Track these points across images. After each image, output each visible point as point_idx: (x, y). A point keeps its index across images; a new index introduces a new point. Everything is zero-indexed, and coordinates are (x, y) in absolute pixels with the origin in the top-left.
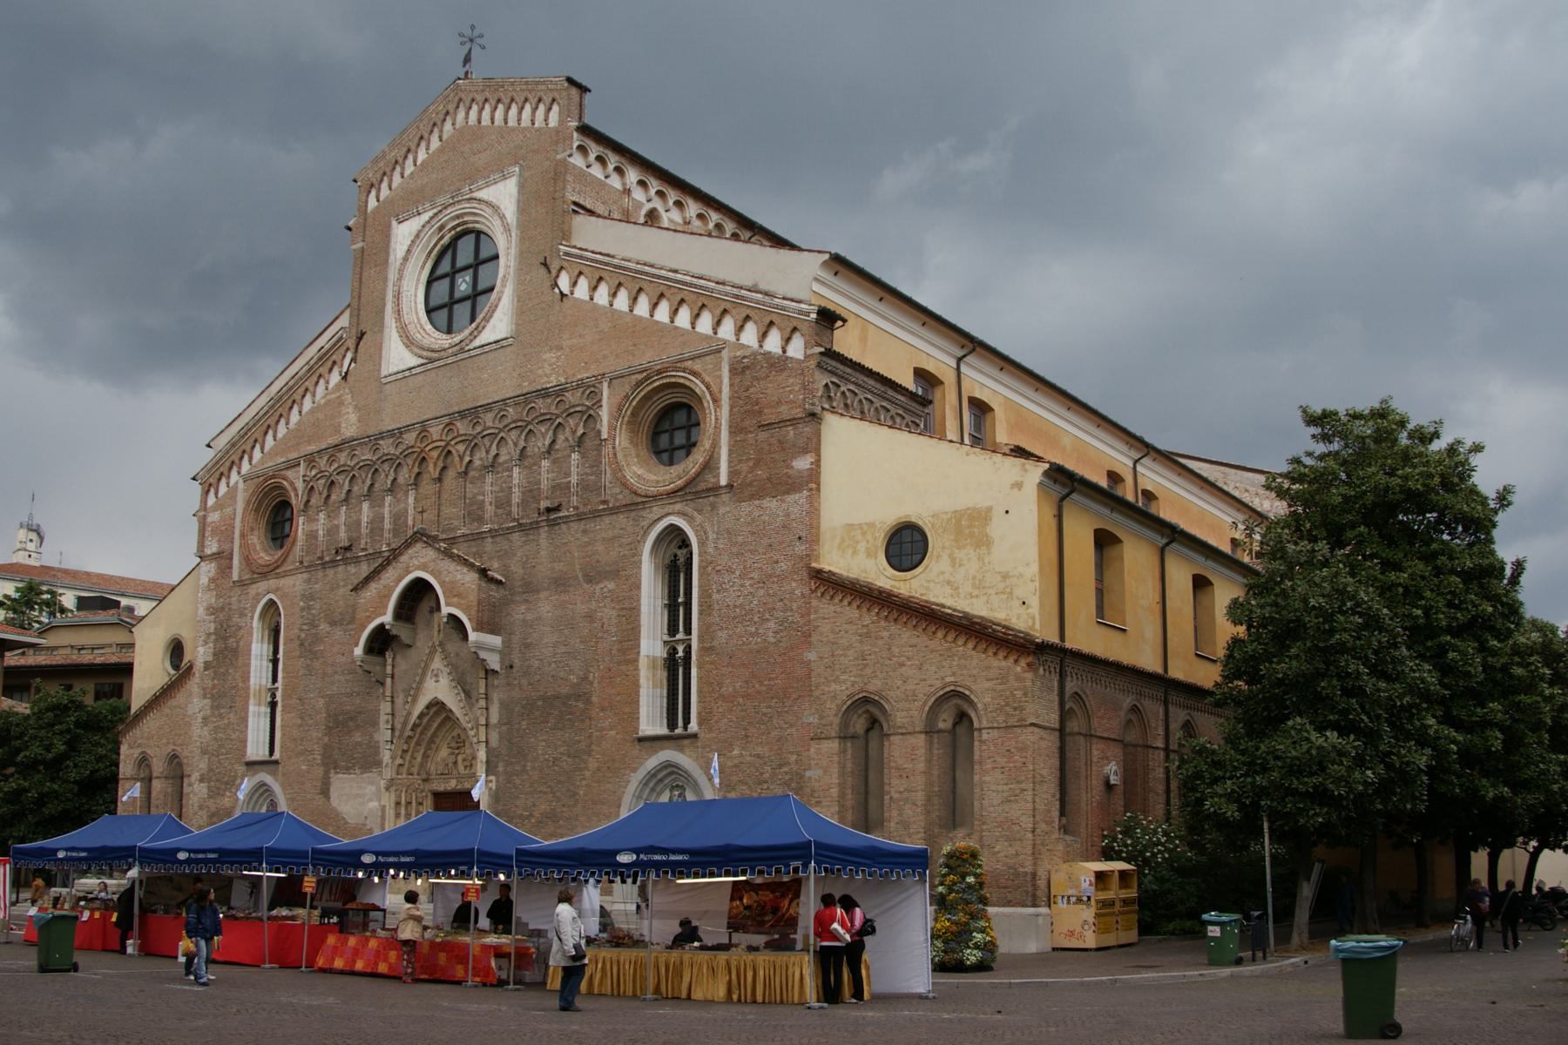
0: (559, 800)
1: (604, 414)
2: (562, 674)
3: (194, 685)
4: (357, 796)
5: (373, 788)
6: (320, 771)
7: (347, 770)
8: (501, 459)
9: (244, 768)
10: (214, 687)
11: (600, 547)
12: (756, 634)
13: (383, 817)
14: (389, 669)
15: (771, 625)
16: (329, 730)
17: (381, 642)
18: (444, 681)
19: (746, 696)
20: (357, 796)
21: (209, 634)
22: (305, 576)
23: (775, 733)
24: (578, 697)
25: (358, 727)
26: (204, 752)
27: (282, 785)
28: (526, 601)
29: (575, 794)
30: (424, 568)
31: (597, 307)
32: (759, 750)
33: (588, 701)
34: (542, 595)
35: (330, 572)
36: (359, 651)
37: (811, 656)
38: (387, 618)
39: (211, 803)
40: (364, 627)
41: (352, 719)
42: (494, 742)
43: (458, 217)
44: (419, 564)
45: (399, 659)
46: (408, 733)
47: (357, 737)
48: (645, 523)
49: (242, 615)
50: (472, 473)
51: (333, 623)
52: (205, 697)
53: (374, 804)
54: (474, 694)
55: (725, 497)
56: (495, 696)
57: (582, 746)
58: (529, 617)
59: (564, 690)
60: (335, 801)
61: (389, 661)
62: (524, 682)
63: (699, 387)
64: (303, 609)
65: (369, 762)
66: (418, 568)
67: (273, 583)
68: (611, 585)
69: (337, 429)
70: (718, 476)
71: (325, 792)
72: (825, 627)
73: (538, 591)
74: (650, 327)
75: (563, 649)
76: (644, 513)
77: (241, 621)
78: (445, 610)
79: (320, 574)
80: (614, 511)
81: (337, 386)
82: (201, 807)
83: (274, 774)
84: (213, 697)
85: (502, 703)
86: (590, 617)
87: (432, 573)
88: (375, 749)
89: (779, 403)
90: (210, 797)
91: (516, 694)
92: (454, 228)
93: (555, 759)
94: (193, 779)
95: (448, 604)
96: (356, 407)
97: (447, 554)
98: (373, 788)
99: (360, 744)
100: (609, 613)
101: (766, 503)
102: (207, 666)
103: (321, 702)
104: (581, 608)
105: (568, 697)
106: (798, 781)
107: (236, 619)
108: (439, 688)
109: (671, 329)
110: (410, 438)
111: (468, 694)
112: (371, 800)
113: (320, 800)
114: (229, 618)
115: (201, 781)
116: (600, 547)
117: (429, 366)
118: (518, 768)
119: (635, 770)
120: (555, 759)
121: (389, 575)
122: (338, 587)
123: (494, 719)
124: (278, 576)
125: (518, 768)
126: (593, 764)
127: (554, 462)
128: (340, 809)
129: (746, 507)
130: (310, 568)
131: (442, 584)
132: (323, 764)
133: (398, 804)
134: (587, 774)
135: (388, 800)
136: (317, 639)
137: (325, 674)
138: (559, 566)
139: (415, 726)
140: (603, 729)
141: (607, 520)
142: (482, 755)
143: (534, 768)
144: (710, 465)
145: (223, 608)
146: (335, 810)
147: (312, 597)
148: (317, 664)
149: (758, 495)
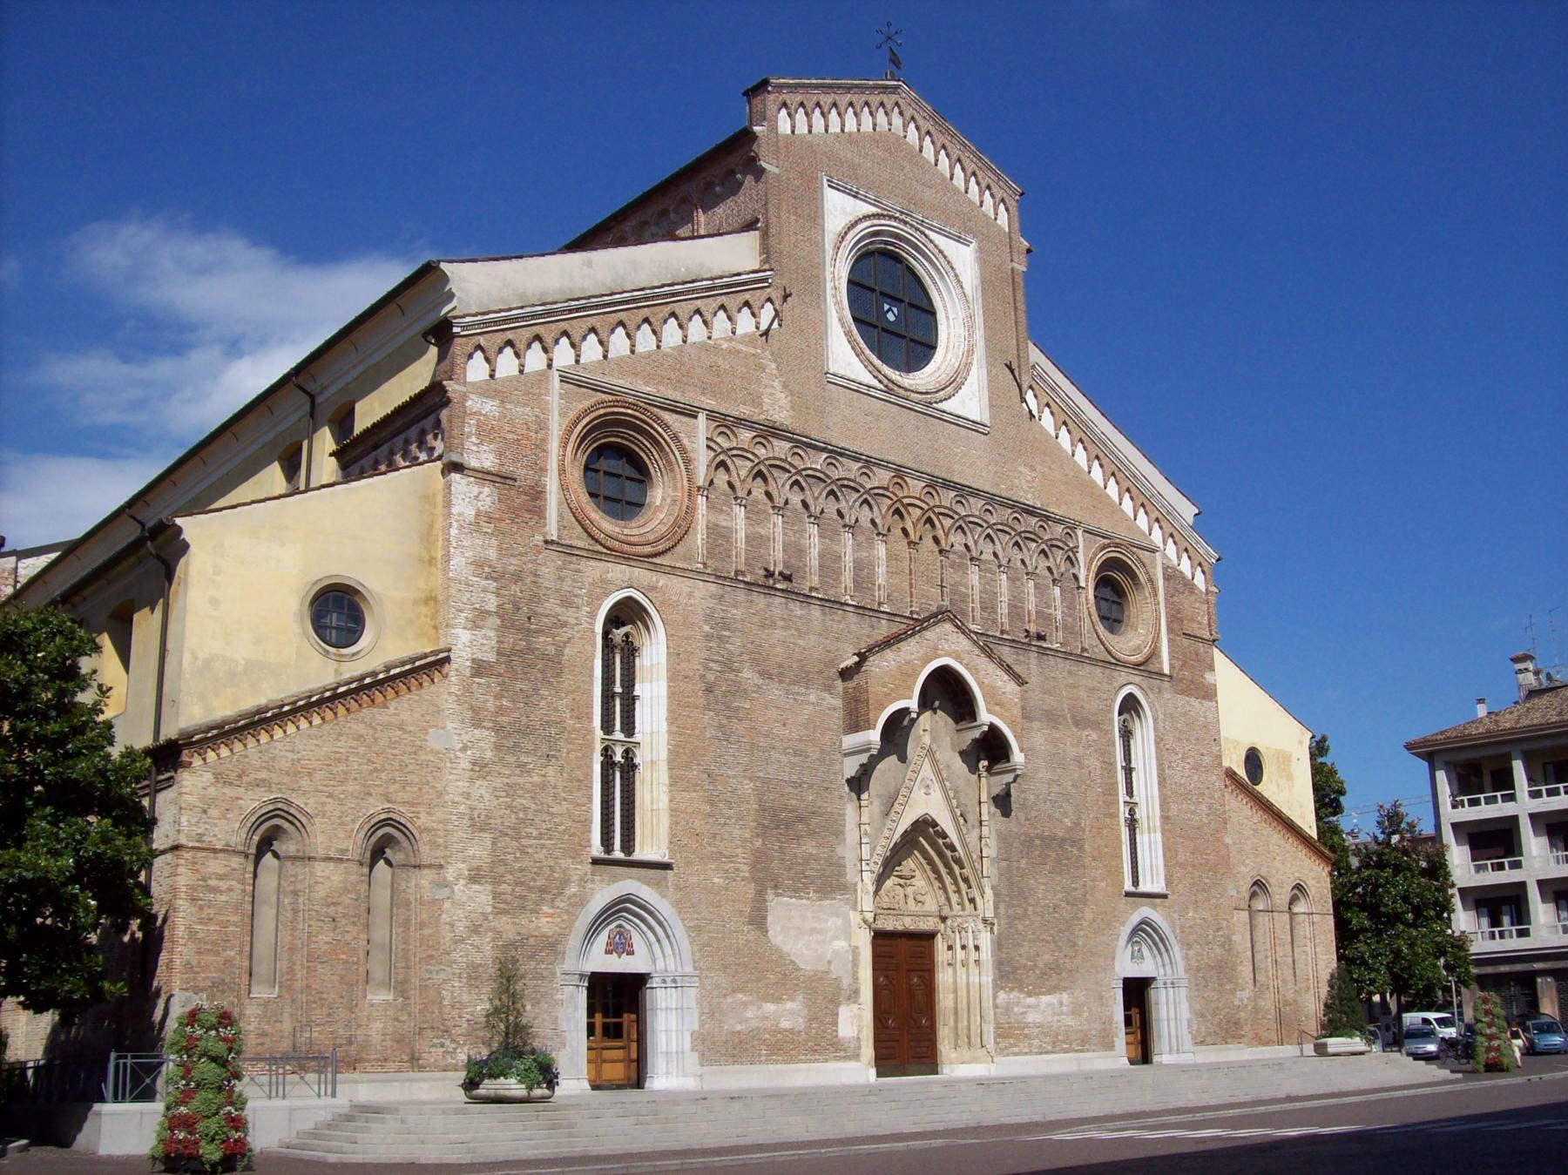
0: (1061, 950)
1: (1081, 556)
2: (1057, 815)
3: (445, 692)
4: (813, 931)
5: (839, 922)
6: (750, 889)
7: (797, 891)
9: (588, 868)
10: (500, 711)
11: (1083, 694)
12: (1194, 813)
13: (855, 964)
15: (1203, 807)
16: (762, 830)
18: (937, 794)
19: (1193, 866)
20: (813, 931)
21: (483, 614)
22: (713, 588)
23: (1213, 901)
24: (1073, 842)
25: (812, 834)
26: (479, 825)
27: (677, 904)
29: (1075, 944)
30: (957, 658)
31: (1059, 448)
32: (1206, 915)
33: (1081, 849)
35: (760, 600)
37: (1228, 840)
38: (913, 704)
39: (505, 925)
41: (800, 819)
43: (897, 236)
44: (948, 649)
47: (810, 847)
48: (1117, 685)
49: (566, 602)
51: (765, 674)
52: (477, 724)
53: (841, 944)
55: (1167, 685)
57: (1078, 894)
59: (1060, 834)
60: (778, 932)
63: (1142, 577)
64: (708, 637)
65: (832, 884)
66: (950, 655)
67: (640, 574)
68: (1094, 736)
69: (756, 400)
70: (1161, 663)
71: (758, 920)
72: (1235, 819)
74: (1100, 497)
75: (1055, 789)
76: (1116, 674)
77: (569, 615)
79: (741, 595)
80: (1094, 662)
81: (748, 339)
82: (475, 929)
83: (658, 885)
84: (498, 729)
86: (1079, 761)
87: (966, 666)
88: (838, 867)
89: (1192, 620)
90: (499, 912)
92: (887, 243)
93: (1056, 906)
94: (450, 873)
95: (989, 711)
96: (785, 386)
97: (987, 651)
98: (839, 922)
100: (1093, 763)
101: (1192, 700)
102: (479, 668)
103: (748, 787)
104: (1071, 751)
105: (1063, 840)
106: (1228, 945)
107: (551, 605)
108: (927, 801)
109: (1117, 508)
110: (882, 477)
112: (835, 938)
113: (751, 934)
114: (534, 598)
115: (475, 877)
116: (1083, 694)
117: (893, 399)
118: (1020, 911)
119: (1123, 924)
120: (1056, 906)
121: (910, 648)
122: (773, 625)
123: (994, 854)
124: (655, 568)
126: (1088, 916)
127: (1036, 586)
128: (786, 948)
129: (1181, 700)
130: (719, 577)
131: (981, 684)
132: (754, 879)
134: (1085, 924)
136: (737, 690)
137: (753, 747)
138: (1049, 700)
140: (1094, 880)
141: (1088, 668)
143: (1035, 913)
144: (1154, 653)
145: (518, 577)
146: (778, 950)
147: (726, 627)
148: (739, 728)
149: (1186, 692)
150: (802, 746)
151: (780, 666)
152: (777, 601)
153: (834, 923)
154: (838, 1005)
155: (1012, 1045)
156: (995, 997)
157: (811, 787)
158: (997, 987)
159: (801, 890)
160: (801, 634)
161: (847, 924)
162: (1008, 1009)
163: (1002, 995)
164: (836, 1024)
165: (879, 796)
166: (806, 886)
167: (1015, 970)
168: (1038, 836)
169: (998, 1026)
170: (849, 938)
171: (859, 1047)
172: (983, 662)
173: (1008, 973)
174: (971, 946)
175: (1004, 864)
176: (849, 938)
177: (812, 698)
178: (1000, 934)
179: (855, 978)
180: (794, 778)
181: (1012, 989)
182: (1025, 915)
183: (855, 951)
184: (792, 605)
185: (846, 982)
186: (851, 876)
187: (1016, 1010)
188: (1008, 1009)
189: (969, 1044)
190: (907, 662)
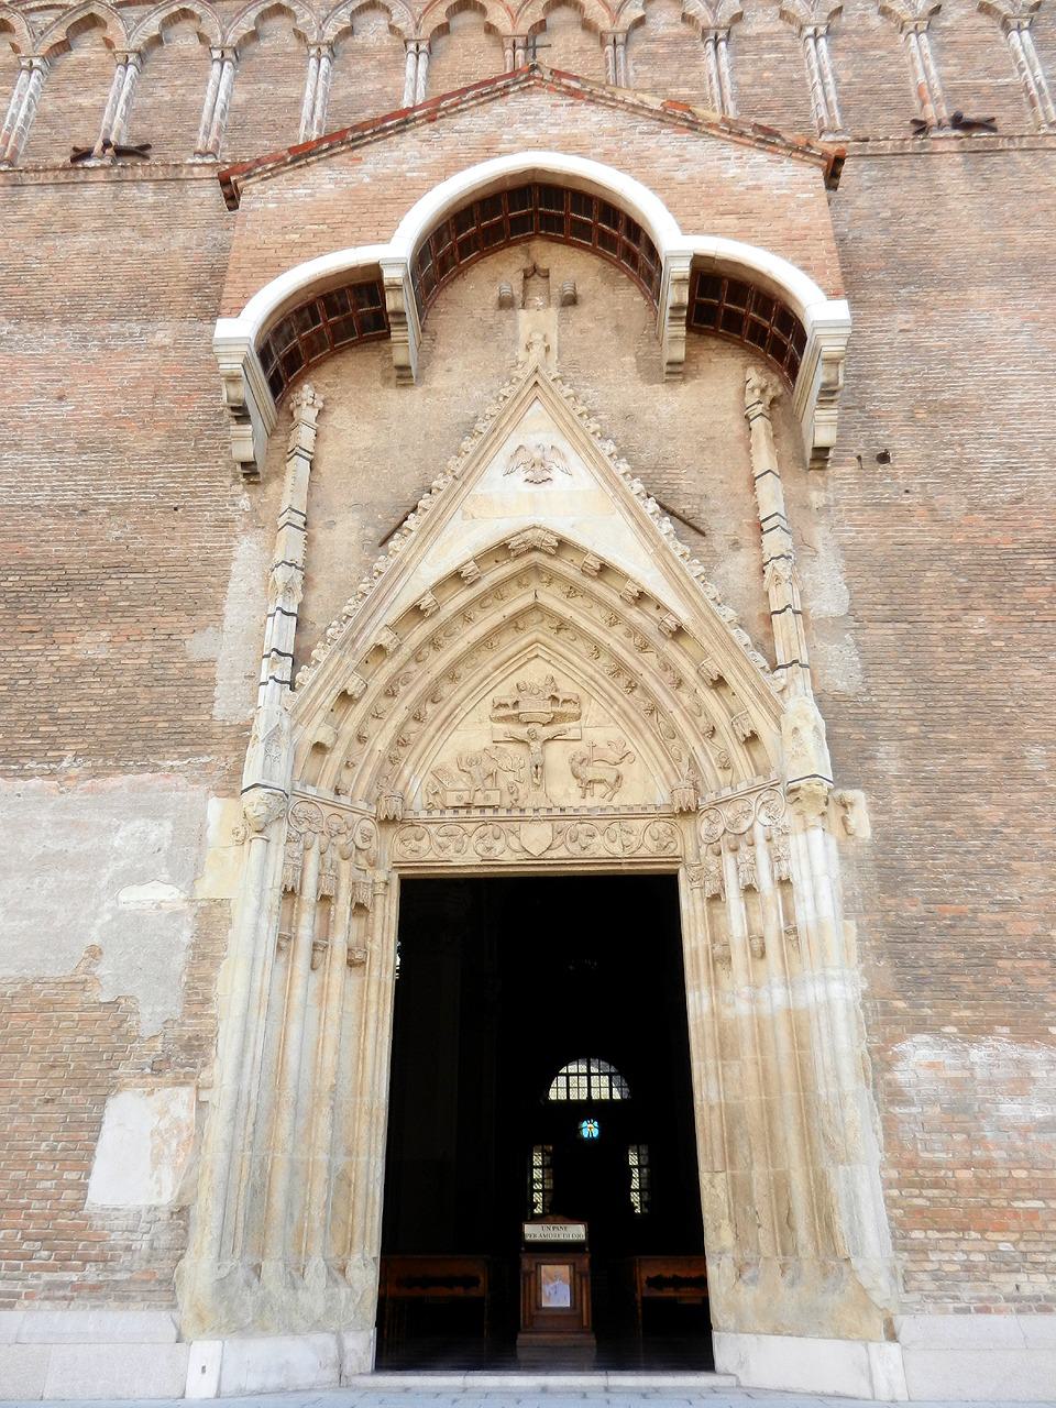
5: (161, 832)
8: (749, 29)
14: (305, 436)
17: (337, 324)
28: (912, 304)
34: (979, 295)
36: (241, 328)
38: (394, 252)
40: (277, 269)
41: (68, 585)
42: (842, 667)
45: (340, 417)
46: (377, 634)
47: (92, 645)
50: (640, 47)
53: (162, 894)
54: (723, 526)
56: (819, 535)
58: (932, 340)
61: (307, 414)
62: (952, 503)
65: (158, 725)
73: (959, 286)
78: (677, 245)
85: (852, 557)
87: (606, 157)
88: (197, 684)
91: (920, 533)
95: (686, 229)
99: (98, 669)
111: (690, 526)
112: (142, 879)
123: (830, 598)
125: (985, 762)
131: (659, 186)
133: (290, 894)
135: (244, 878)
139: (416, 611)
142: (803, 710)
150: (108, 432)
151: (74, 294)
152: (89, 192)
153: (129, 836)
154: (101, 1089)
155: (1007, 1265)
156: (880, 1062)
157: (118, 510)
158: (886, 1024)
159: (31, 753)
160: (146, 235)
161: (194, 836)
162: (961, 1110)
163: (919, 1058)
164: (83, 1159)
165: (357, 506)
166: (52, 742)
167: (985, 959)
168: (1033, 548)
169: (908, 1173)
170: (188, 870)
171: (179, 1249)
172: (668, 145)
173: (930, 962)
174: (766, 884)
175: (887, 630)
176: (188, 870)
177: (163, 337)
178: (886, 838)
179: (198, 997)
180: (69, 497)
181: (974, 1031)
182: (1012, 771)
183: (210, 921)
184: (130, 192)
185: (153, 1014)
186: (225, 707)
187: (1010, 1109)
188: (961, 1110)
189: (787, 1248)
190: (387, 178)
